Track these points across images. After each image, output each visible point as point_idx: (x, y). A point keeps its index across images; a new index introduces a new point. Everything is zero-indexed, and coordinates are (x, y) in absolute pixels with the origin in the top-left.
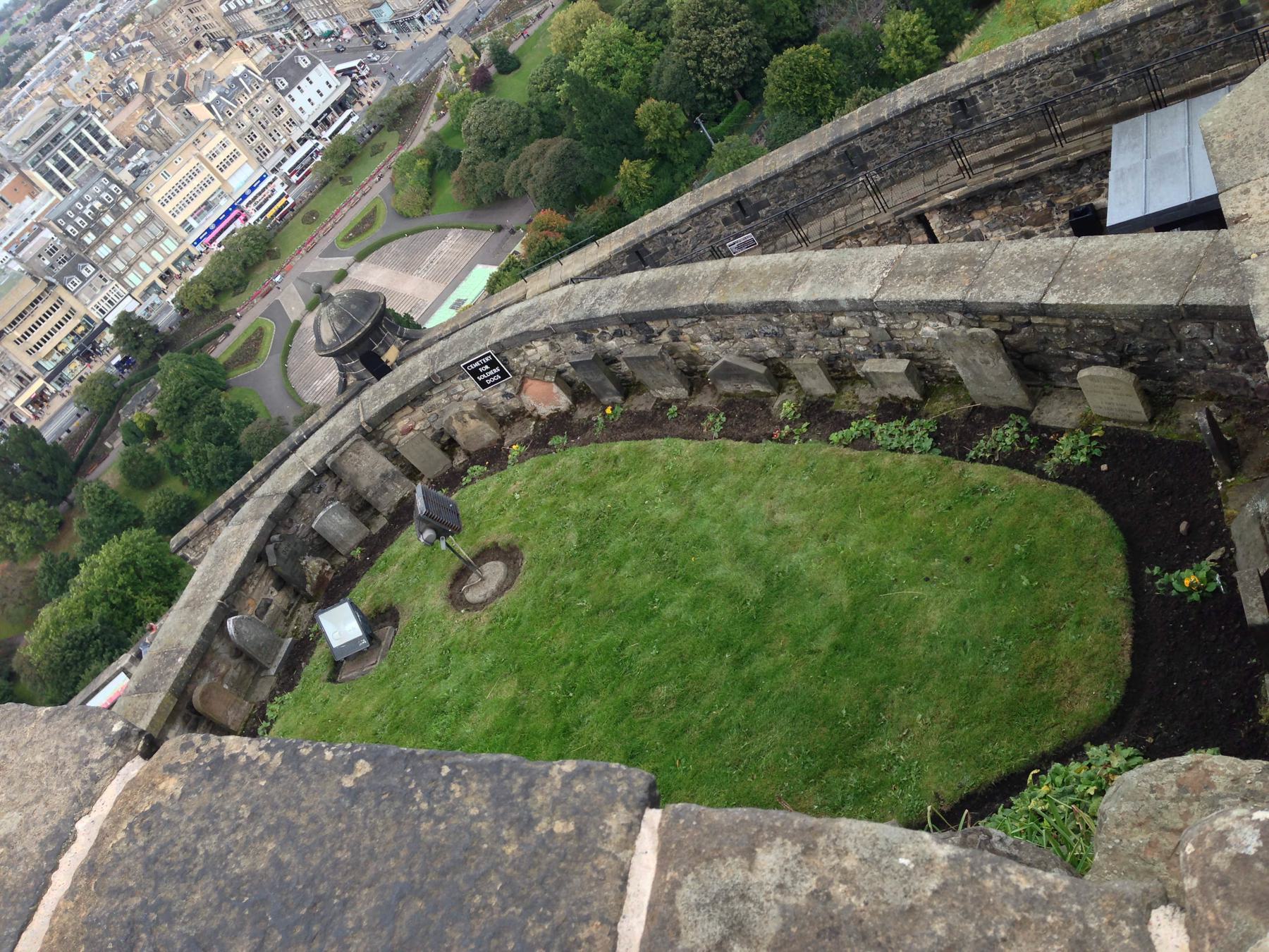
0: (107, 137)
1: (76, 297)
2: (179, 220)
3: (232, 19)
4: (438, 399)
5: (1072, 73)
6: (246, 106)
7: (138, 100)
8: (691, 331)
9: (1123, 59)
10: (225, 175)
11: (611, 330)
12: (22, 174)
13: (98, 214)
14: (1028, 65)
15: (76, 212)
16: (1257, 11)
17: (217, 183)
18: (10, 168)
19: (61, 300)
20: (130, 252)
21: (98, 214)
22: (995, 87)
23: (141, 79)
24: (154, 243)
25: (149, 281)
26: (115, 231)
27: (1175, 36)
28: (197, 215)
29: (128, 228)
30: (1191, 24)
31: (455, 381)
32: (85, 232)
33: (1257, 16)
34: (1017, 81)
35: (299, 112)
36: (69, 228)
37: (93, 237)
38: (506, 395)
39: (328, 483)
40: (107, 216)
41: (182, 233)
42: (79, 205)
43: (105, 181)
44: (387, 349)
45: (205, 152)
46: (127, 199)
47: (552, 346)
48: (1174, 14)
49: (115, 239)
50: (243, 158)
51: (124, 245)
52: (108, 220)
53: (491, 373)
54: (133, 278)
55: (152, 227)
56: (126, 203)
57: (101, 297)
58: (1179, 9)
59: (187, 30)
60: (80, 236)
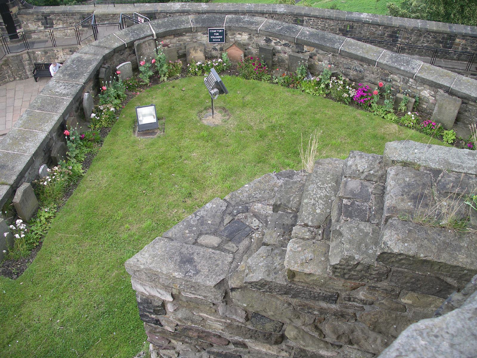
4: (187, 38)
5: (338, 29)
8: (321, 57)
9: (355, 33)
11: (283, 42)
14: (327, 19)
16: (400, 38)
22: (312, 20)
27: (374, 34)
30: (380, 32)
31: (199, 34)
33: (400, 40)
34: (320, 22)
38: (215, 49)
39: (127, 52)
44: (14, 6)
47: (250, 38)
48: (377, 26)
53: (218, 37)
58: (379, 25)
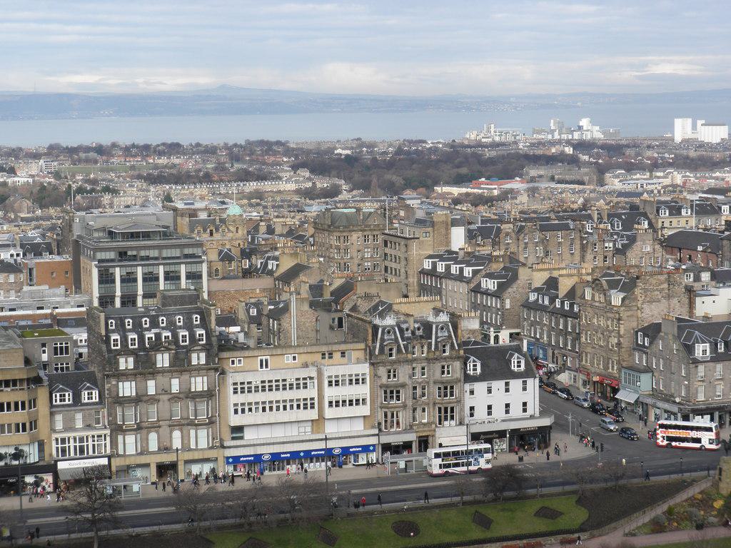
1: (52, 414)
2: (235, 420)
3: (427, 281)
6: (415, 360)
7: (267, 282)
10: (329, 413)
12: (76, 264)
13: (157, 345)
15: (138, 327)
17: (314, 414)
19: (33, 403)
20: (153, 413)
21: (157, 345)
23: (287, 264)
24: (187, 424)
25: (143, 460)
26: (159, 377)
32: (126, 351)
35: (467, 411)
36: (115, 336)
37: (131, 366)
40: (166, 356)
41: (227, 435)
43: (196, 319)
45: (330, 371)
46: (203, 355)
49: (151, 387)
50: (365, 410)
51: (153, 400)
52: (163, 360)
54: (129, 444)
55: (202, 407)
56: (198, 358)
57: (78, 434)
59: (356, 261)
60: (119, 353)
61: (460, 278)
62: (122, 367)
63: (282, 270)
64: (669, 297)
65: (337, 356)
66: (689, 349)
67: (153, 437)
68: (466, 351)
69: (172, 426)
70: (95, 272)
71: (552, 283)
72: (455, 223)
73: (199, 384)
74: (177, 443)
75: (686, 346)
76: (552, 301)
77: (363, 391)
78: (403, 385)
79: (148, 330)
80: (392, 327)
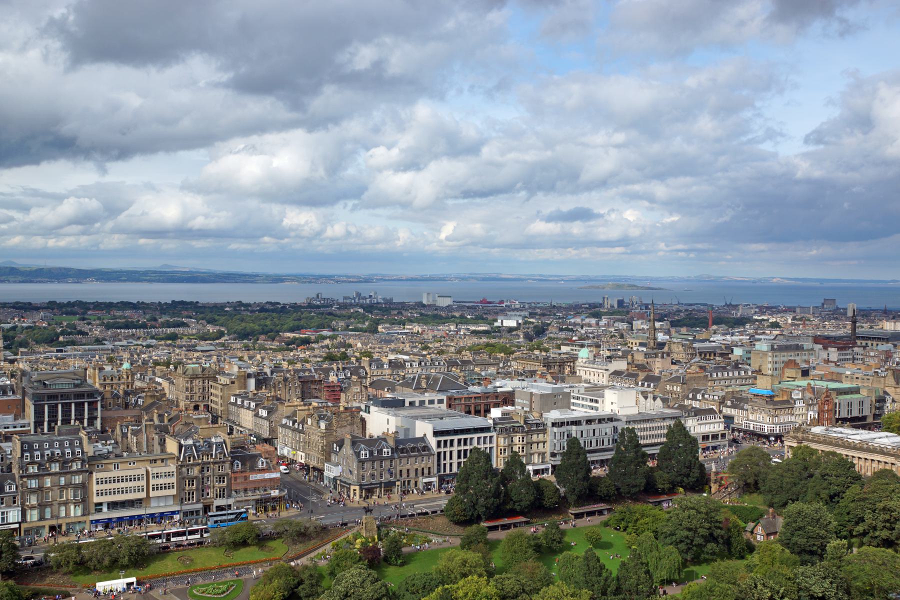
0: (96, 418)
2: (96, 499)
3: (233, 408)
15: (41, 449)
17: (143, 495)
18: (20, 392)
23: (150, 401)
24: (66, 503)
28: (113, 505)
29: (63, 481)
41: (92, 509)
42: (46, 445)
45: (155, 471)
61: (249, 408)
62: (31, 471)
63: (146, 404)
64: (352, 424)
65: (159, 462)
66: (358, 454)
67: (48, 510)
68: (232, 457)
69: (60, 504)
70: (32, 407)
71: (295, 414)
72: (249, 376)
73: (78, 479)
74: (63, 514)
75: (355, 452)
76: (294, 424)
77: (173, 480)
78: (196, 478)
79: (47, 449)
80: (190, 446)
